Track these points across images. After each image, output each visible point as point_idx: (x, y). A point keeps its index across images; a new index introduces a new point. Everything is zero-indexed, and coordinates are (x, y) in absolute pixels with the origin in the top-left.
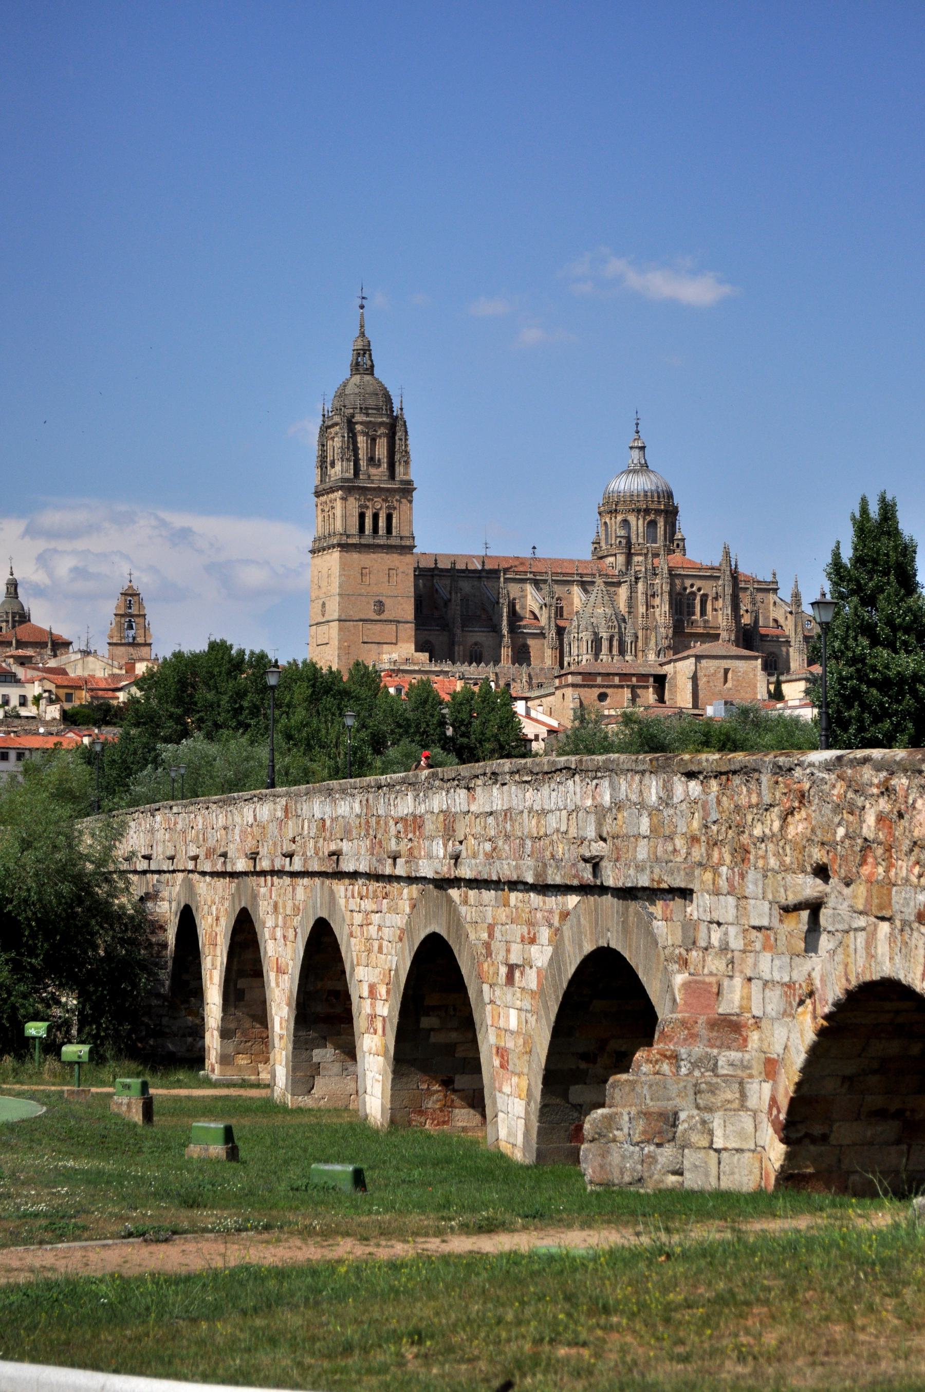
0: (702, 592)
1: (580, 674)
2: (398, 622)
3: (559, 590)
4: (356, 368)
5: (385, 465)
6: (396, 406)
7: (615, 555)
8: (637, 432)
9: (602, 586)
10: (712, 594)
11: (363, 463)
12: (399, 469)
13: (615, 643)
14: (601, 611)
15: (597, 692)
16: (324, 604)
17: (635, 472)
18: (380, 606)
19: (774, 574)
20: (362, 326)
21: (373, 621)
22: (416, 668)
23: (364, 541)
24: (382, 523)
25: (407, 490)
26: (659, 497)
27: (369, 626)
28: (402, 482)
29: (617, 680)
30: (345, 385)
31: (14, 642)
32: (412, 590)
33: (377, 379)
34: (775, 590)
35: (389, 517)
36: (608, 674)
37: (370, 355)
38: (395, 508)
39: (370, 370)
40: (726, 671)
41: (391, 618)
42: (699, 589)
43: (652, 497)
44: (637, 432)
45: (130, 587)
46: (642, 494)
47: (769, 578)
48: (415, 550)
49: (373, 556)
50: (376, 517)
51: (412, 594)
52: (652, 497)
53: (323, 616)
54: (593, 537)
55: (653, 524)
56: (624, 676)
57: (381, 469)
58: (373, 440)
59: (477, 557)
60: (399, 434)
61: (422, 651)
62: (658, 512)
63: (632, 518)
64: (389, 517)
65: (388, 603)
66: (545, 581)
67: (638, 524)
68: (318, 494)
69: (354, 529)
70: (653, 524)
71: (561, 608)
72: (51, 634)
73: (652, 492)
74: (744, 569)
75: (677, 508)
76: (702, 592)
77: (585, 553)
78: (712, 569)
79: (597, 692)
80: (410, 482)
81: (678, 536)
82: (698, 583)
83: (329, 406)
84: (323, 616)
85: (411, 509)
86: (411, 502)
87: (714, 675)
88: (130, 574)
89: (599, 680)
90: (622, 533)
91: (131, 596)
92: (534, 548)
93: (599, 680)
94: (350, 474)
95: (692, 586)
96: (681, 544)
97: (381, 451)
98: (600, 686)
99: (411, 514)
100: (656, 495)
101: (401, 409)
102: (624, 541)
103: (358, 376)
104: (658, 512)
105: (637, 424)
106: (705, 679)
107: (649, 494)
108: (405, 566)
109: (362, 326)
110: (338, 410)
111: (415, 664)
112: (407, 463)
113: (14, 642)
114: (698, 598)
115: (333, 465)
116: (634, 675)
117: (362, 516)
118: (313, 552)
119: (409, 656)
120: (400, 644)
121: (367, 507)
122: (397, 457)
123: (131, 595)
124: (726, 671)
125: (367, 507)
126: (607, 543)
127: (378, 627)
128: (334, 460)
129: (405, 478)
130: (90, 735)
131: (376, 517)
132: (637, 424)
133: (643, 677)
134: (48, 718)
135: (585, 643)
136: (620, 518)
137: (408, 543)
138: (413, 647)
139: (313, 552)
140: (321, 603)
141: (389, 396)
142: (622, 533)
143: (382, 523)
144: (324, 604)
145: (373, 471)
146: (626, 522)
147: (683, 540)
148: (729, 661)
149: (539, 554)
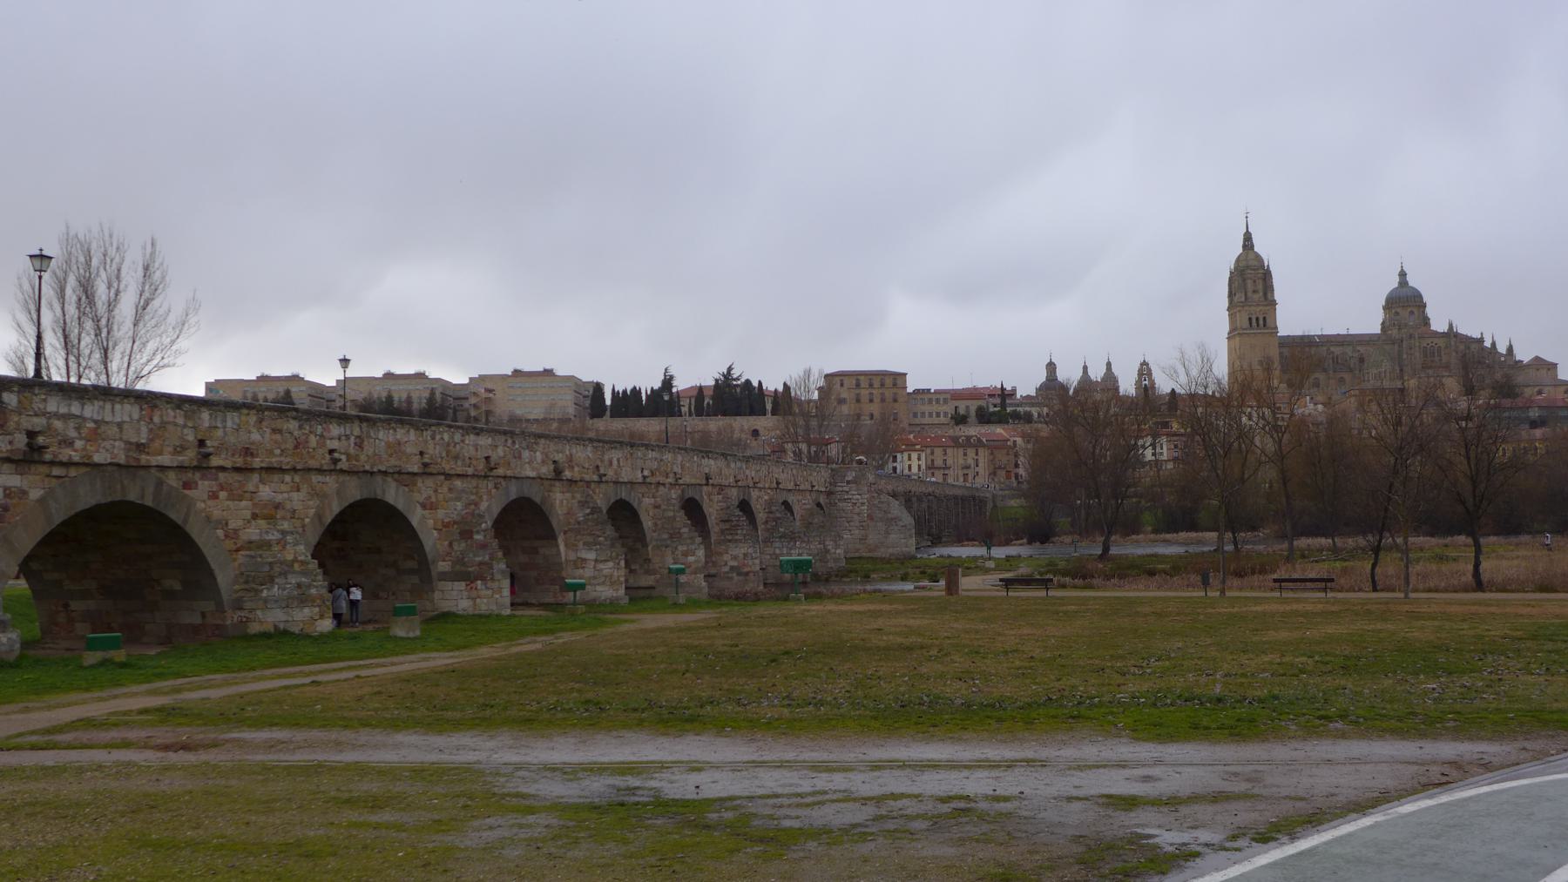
4: (1244, 246)
5: (1261, 294)
6: (1266, 264)
11: (1249, 294)
12: (1269, 295)
19: (1482, 334)
24: (1261, 322)
35: (1264, 318)
45: (1144, 361)
47: (1479, 336)
50: (1257, 319)
59: (1318, 336)
64: (1264, 318)
69: (1246, 323)
80: (1275, 301)
82: (1436, 341)
83: (1232, 267)
91: (1144, 363)
94: (1243, 299)
97: (1260, 287)
115: (1235, 294)
117: (1250, 319)
131: (1257, 319)
143: (1261, 322)
145: (1256, 297)
146: (1397, 313)
149: (1351, 332)
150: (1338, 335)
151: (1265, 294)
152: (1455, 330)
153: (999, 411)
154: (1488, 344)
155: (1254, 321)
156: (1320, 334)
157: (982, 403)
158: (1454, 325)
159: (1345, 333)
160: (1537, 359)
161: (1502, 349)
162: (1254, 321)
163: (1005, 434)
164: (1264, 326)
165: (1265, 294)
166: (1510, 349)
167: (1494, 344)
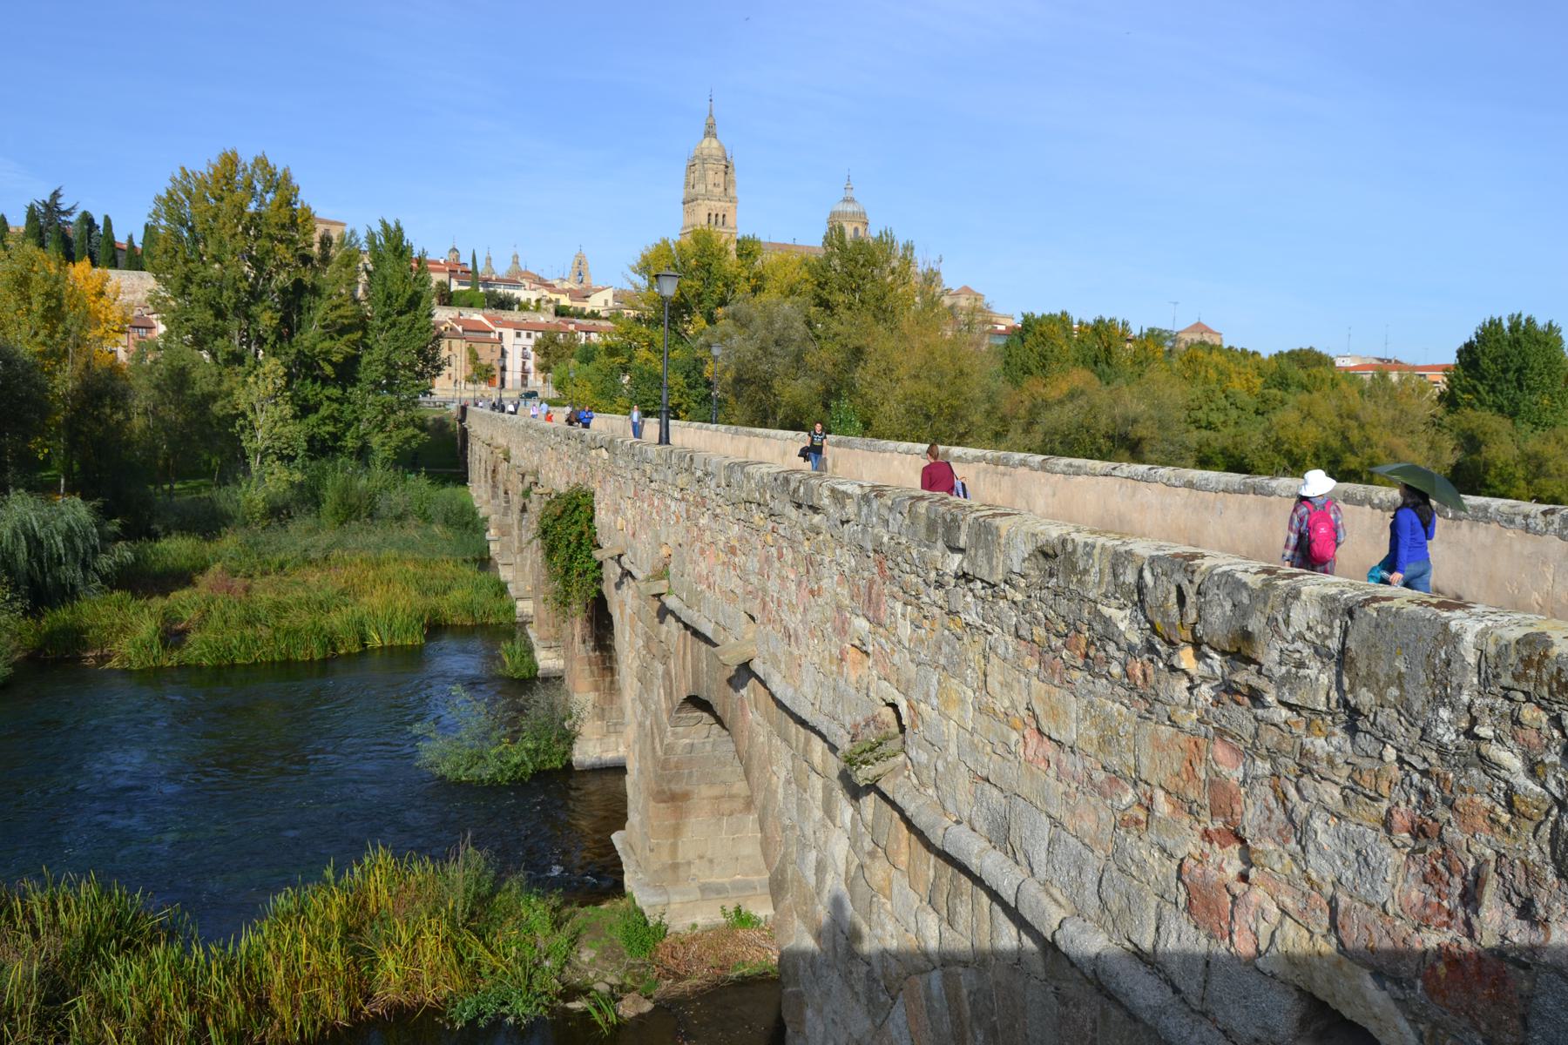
5: (722, 189)
11: (710, 187)
12: (730, 191)
24: (720, 219)
60: (730, 170)
97: (720, 178)
143: (720, 219)
155: (713, 218)
157: (444, 277)
162: (713, 218)
163: (486, 322)
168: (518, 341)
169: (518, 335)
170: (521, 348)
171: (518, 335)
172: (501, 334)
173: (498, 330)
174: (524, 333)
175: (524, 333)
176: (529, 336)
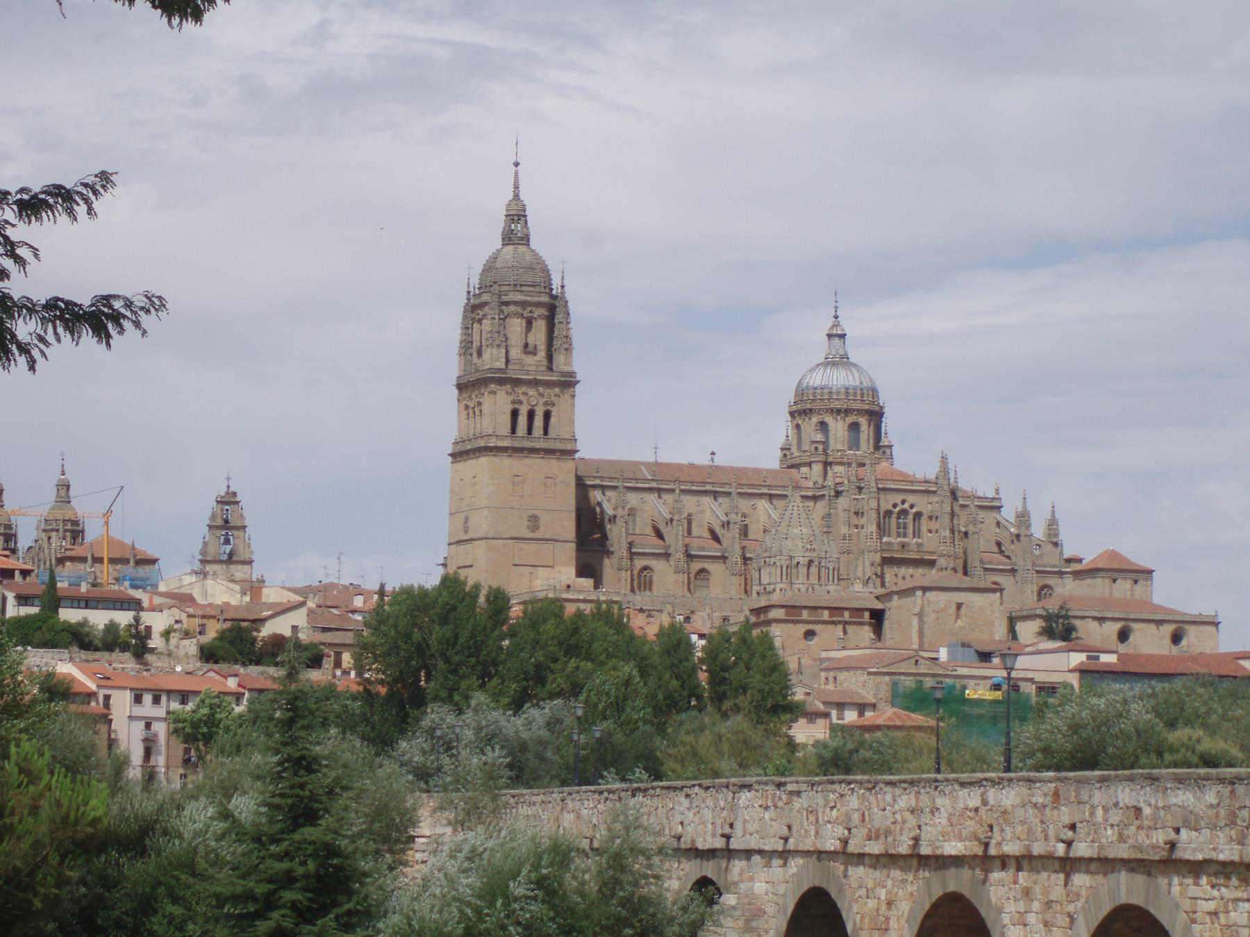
0: (914, 510)
1: (783, 607)
2: (556, 541)
3: (744, 505)
4: (509, 238)
5: (542, 354)
6: (556, 283)
7: (809, 464)
8: (836, 317)
9: (799, 500)
10: (926, 512)
11: (515, 353)
12: (559, 359)
13: (836, 572)
14: (797, 531)
15: (802, 628)
16: (466, 519)
17: (834, 364)
18: (534, 521)
20: (516, 187)
21: (528, 539)
22: (581, 597)
23: (518, 444)
24: (538, 422)
25: (568, 383)
26: (862, 395)
27: (523, 546)
28: (563, 374)
29: (826, 615)
30: (495, 258)
31: (90, 558)
32: (573, 502)
33: (533, 251)
34: (999, 508)
35: (547, 416)
36: (816, 608)
37: (526, 222)
38: (553, 405)
39: (525, 240)
40: (959, 606)
41: (547, 536)
42: (912, 506)
43: (855, 394)
44: (836, 317)
46: (843, 391)
47: (991, 494)
48: (577, 456)
49: (527, 461)
50: (531, 415)
51: (573, 508)
52: (855, 394)
53: (466, 532)
54: (781, 441)
55: (854, 427)
56: (835, 610)
57: (538, 358)
58: (529, 323)
59: (646, 464)
60: (559, 317)
61: (586, 576)
62: (860, 412)
63: (828, 419)
64: (547, 416)
65: (544, 518)
66: (728, 494)
67: (838, 428)
68: (461, 387)
69: (505, 429)
70: (854, 427)
71: (746, 526)
72: (133, 547)
73: (855, 389)
74: (965, 484)
75: (882, 408)
76: (914, 510)
77: (771, 460)
78: (926, 482)
79: (802, 628)
80: (572, 374)
81: (884, 442)
82: (911, 499)
83: (475, 281)
84: (466, 532)
85: (573, 405)
86: (573, 396)
87: (944, 610)
88: (228, 479)
89: (805, 614)
90: (819, 437)
92: (713, 454)
93: (805, 614)
95: (903, 502)
96: (888, 451)
97: (538, 335)
98: (807, 622)
99: (573, 412)
100: (859, 392)
101: (563, 287)
102: (821, 447)
103: (511, 247)
104: (860, 412)
105: (836, 308)
106: (933, 616)
107: (851, 391)
108: (564, 472)
109: (516, 187)
110: (484, 287)
111: (580, 592)
112: (569, 350)
113: (90, 558)
114: (910, 517)
116: (846, 609)
117: (515, 414)
118: (453, 455)
119: (570, 582)
120: (558, 568)
121: (521, 403)
122: (556, 343)
123: (228, 503)
124: (959, 606)
125: (521, 403)
126: (799, 448)
127: (531, 547)
128: (481, 346)
129: (566, 369)
130: (236, 675)
131: (531, 415)
132: (836, 308)
133: (857, 611)
134: (181, 653)
135: (779, 570)
136: (815, 419)
137: (569, 447)
138: (573, 571)
139: (453, 455)
140: (463, 515)
141: (548, 271)
142: (819, 437)
143: (538, 422)
144: (466, 519)
145: (530, 360)
146: (823, 426)
147: (890, 447)
148: (962, 594)
149: (719, 461)
150: (692, 466)
151: (550, 358)
152: (952, 481)
153: (35, 616)
154: (1008, 513)
155: (522, 421)
156: (652, 460)
158: (951, 466)
159: (703, 460)
160: (1113, 555)
161: (1038, 530)
162: (522, 421)
164: (546, 432)
165: (550, 358)
166: (1052, 525)
167: (1023, 518)
168: (138, 711)
169: (138, 699)
170: (142, 724)
171: (138, 699)
172: (107, 698)
173: (102, 693)
174: (148, 698)
175: (148, 698)
176: (156, 700)
